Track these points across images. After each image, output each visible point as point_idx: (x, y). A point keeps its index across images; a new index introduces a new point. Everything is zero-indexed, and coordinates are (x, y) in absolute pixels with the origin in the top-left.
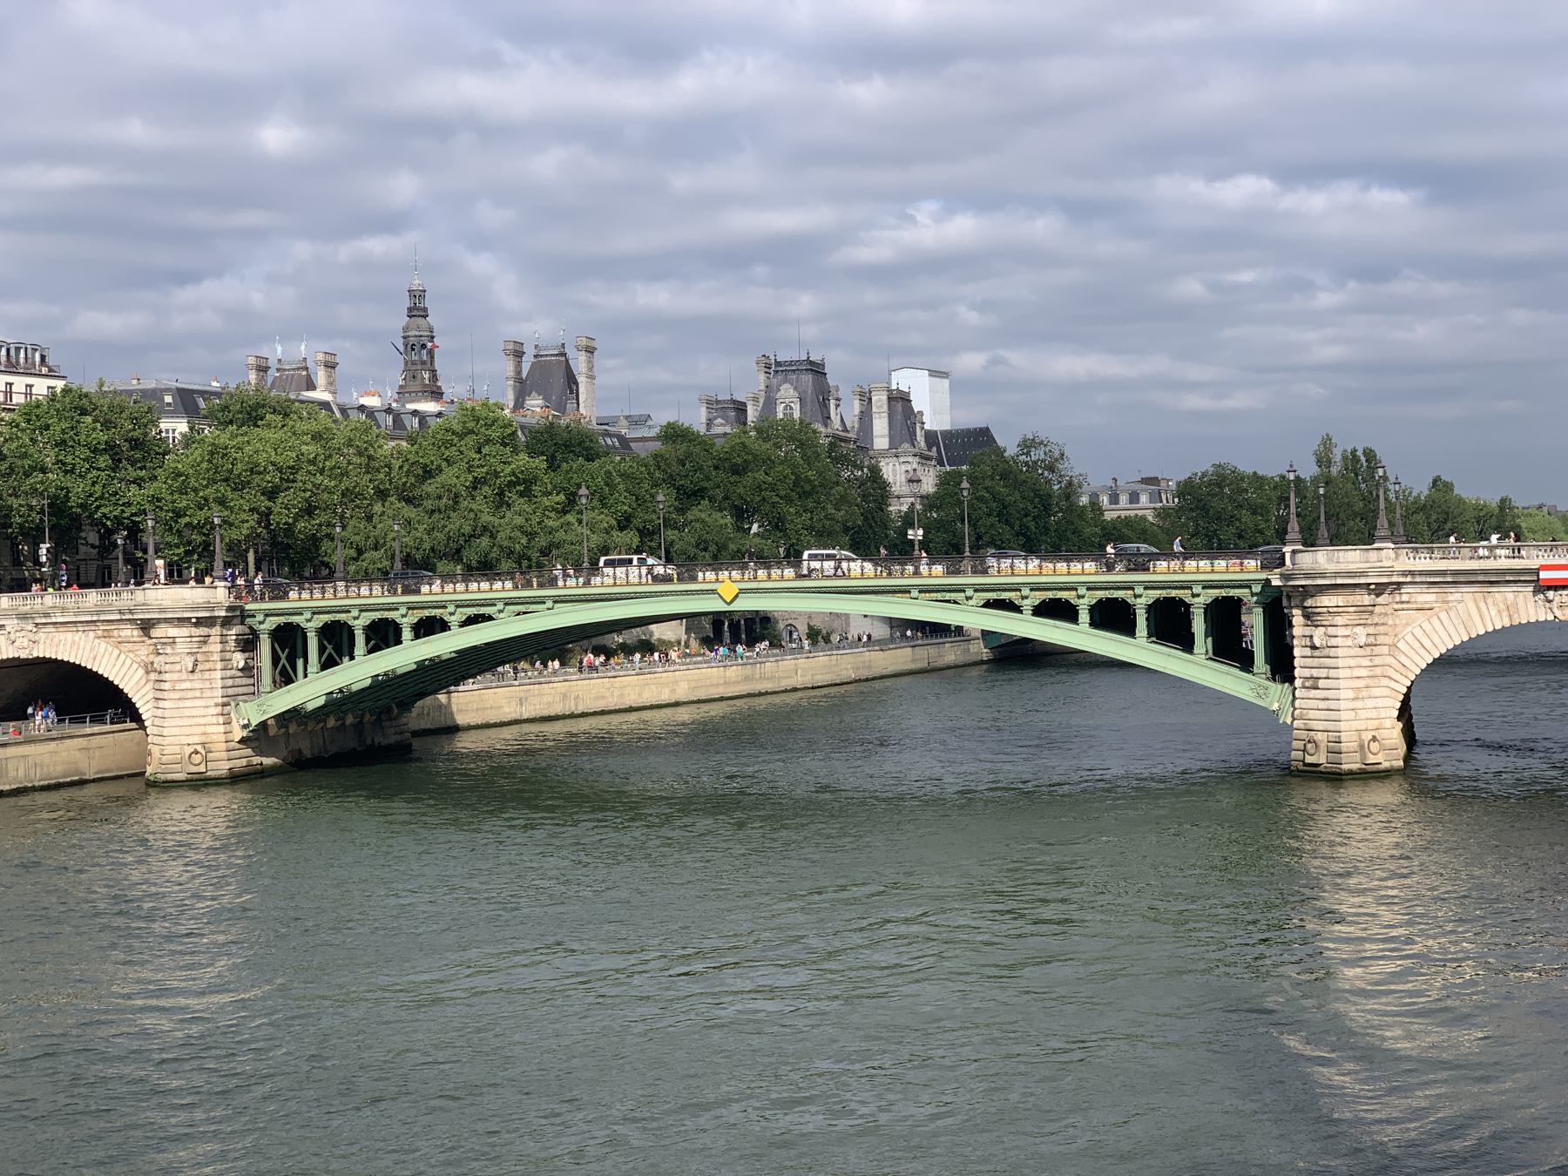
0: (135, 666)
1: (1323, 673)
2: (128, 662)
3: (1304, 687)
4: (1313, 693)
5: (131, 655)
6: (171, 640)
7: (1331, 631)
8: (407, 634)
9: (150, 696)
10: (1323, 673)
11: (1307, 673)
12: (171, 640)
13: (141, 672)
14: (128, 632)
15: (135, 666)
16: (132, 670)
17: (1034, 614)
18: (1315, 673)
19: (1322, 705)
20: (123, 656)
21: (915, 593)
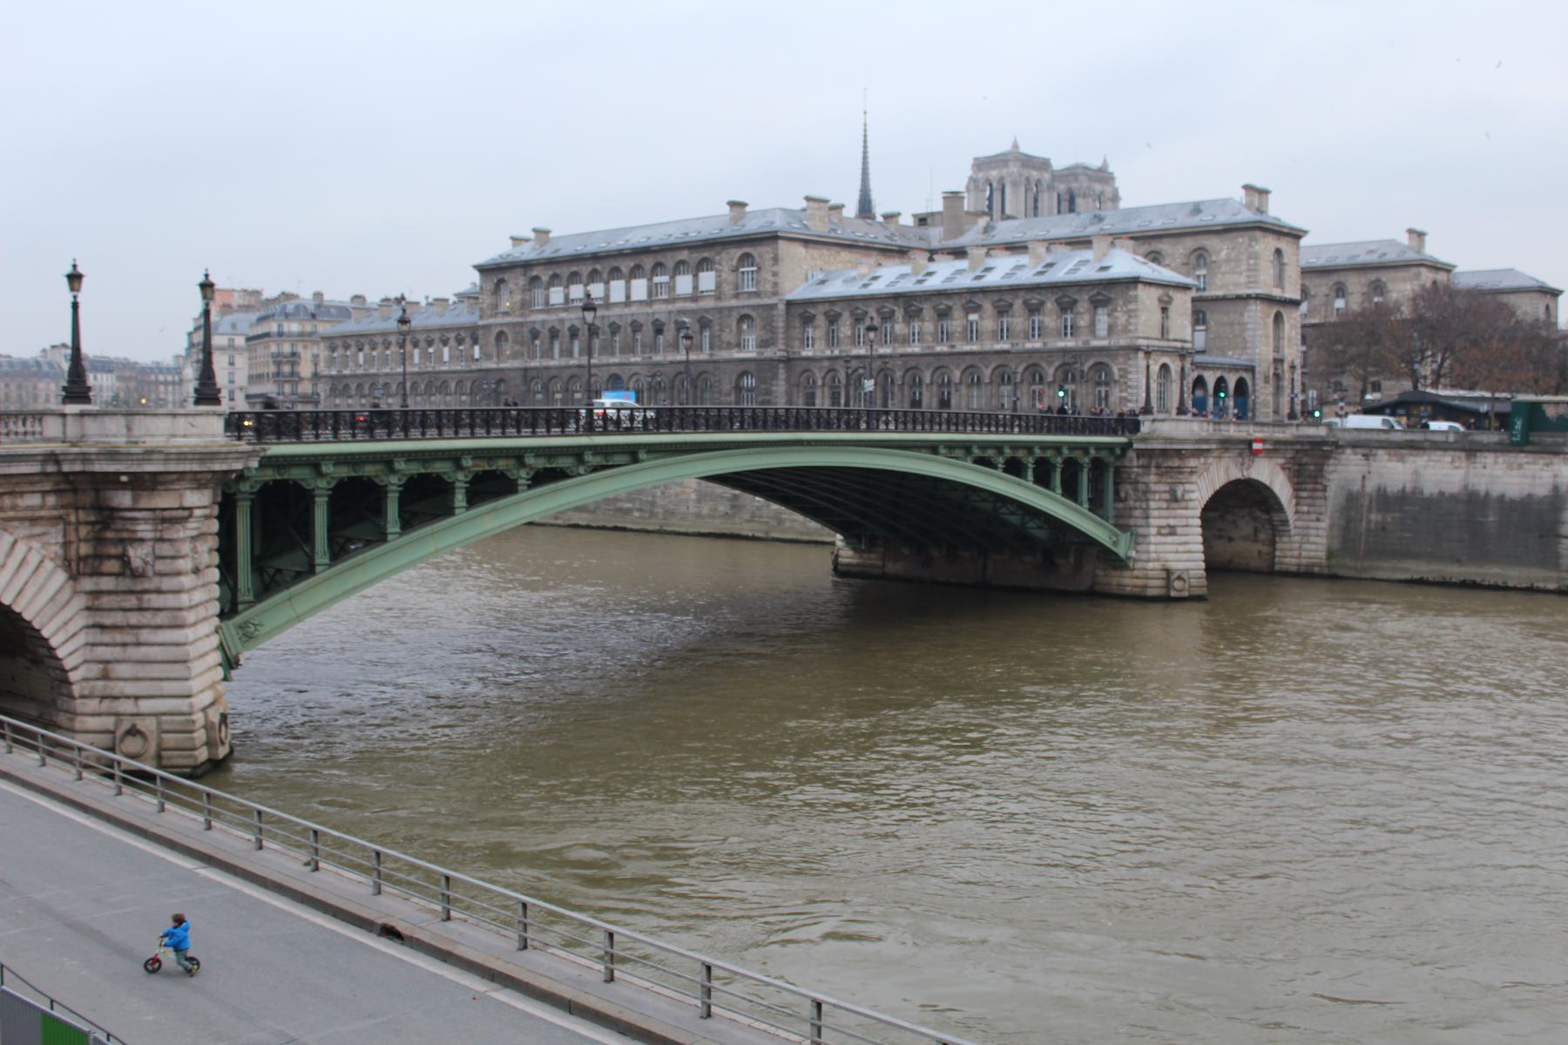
0: (49, 565)
1: (1183, 522)
2: (34, 559)
3: (1159, 534)
4: (1170, 539)
5: (36, 544)
6: (186, 513)
7: (1188, 487)
8: (460, 499)
9: (82, 620)
10: (1183, 522)
11: (1163, 522)
12: (186, 513)
13: (61, 576)
14: (35, 500)
15: (49, 565)
16: (42, 574)
17: (1005, 471)
18: (1172, 522)
19: (1181, 548)
20: (21, 549)
21: (942, 450)
